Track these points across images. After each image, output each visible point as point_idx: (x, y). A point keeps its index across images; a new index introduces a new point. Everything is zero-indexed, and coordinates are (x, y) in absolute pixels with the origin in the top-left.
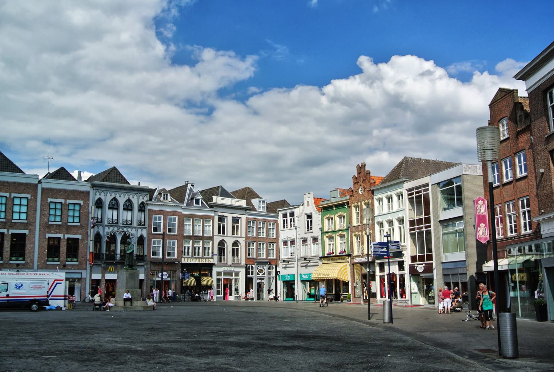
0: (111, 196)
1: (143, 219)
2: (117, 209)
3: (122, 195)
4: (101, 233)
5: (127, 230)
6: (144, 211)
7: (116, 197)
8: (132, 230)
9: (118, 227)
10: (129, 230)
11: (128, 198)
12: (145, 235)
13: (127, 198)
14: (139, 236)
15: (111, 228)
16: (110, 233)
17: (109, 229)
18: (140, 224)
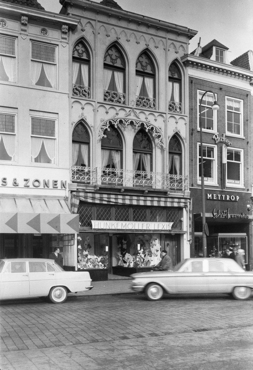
0: (108, 36)
1: (177, 100)
2: (122, 70)
3: (133, 40)
4: (90, 121)
5: (146, 118)
6: (179, 80)
7: (120, 41)
8: (156, 120)
9: (128, 110)
10: (151, 119)
11: (145, 47)
12: (184, 133)
13: (142, 47)
14: (171, 134)
15: (112, 113)
16: (110, 122)
17: (107, 113)
18: (172, 107)
